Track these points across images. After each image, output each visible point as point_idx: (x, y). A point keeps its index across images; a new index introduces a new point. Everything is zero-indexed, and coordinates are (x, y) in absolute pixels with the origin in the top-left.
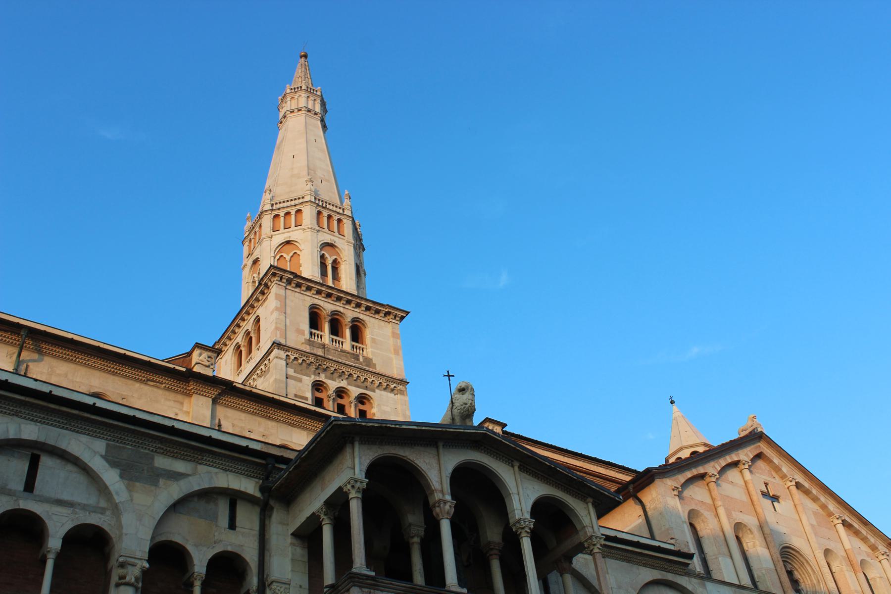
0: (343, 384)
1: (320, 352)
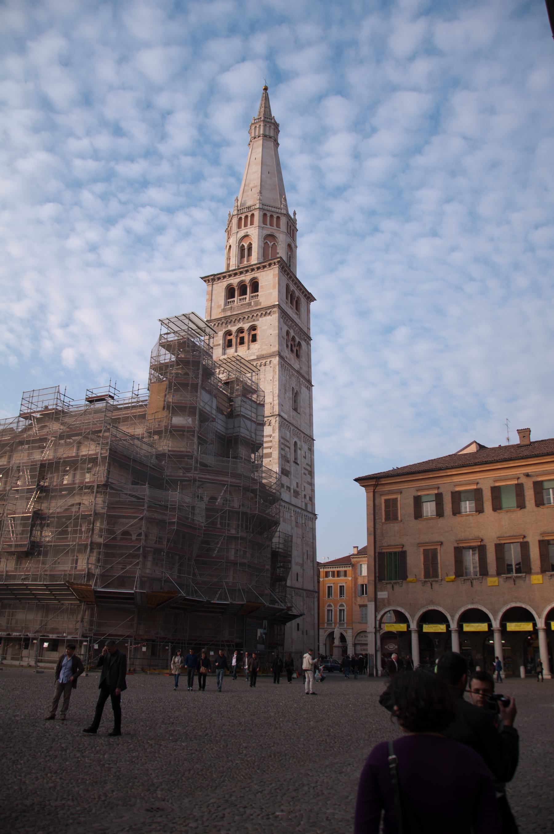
0: (240, 325)
1: (229, 313)
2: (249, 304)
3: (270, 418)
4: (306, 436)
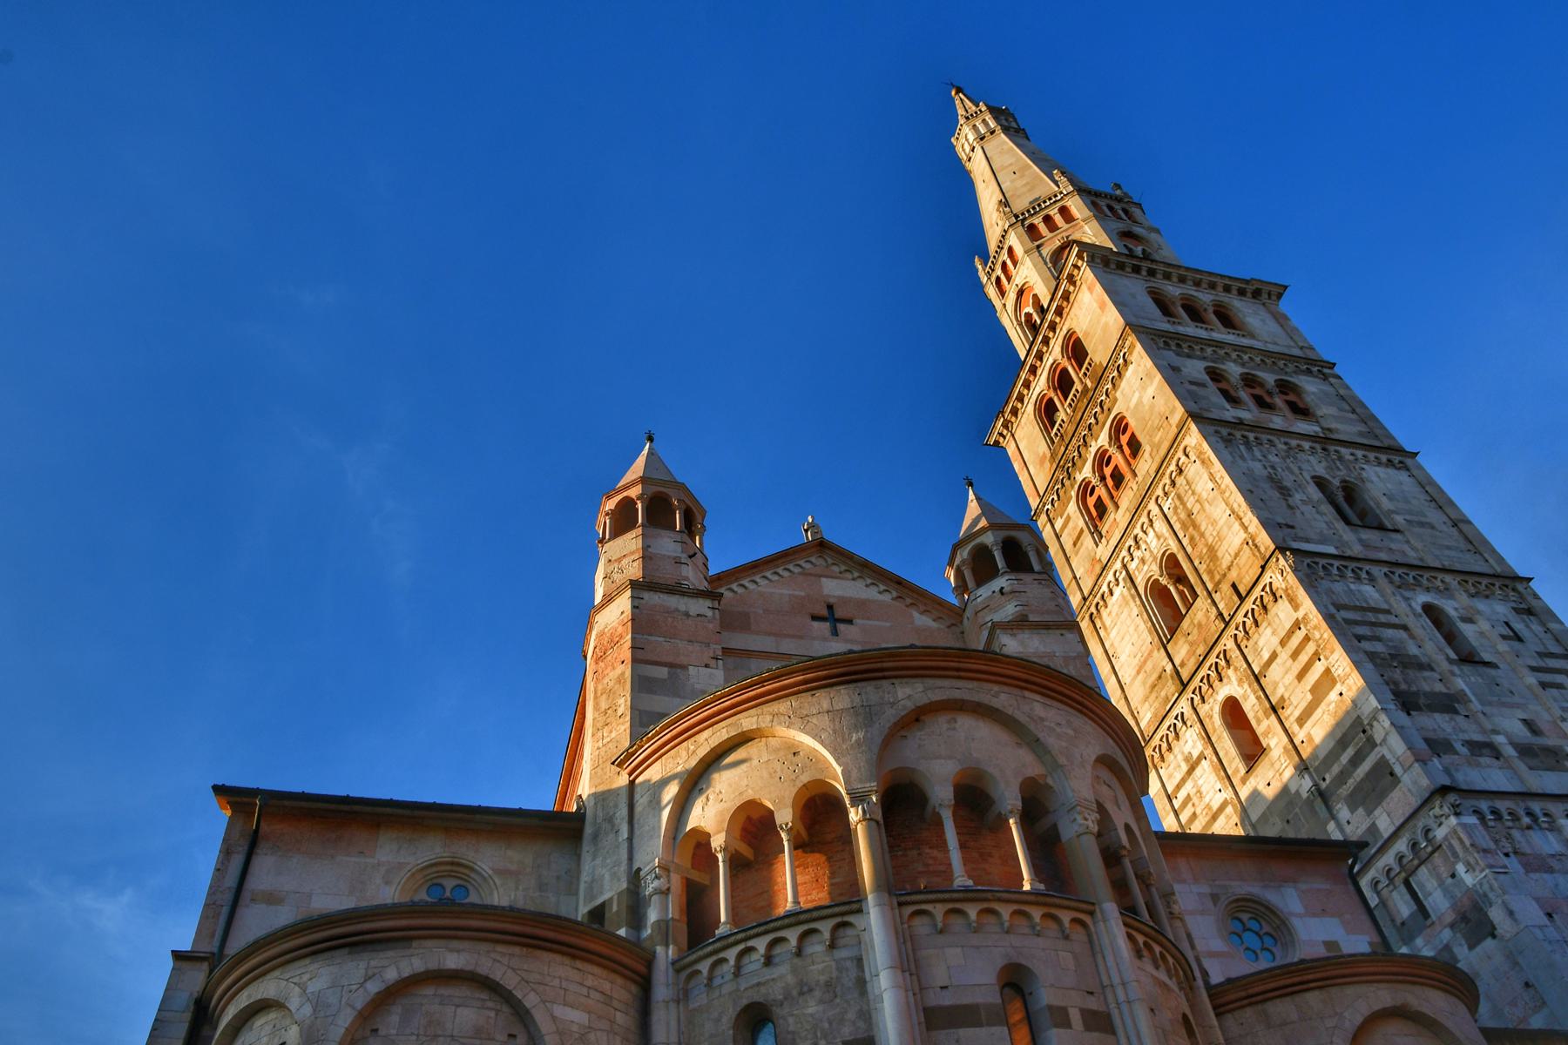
0: (1093, 450)
2: (1086, 389)
3: (1266, 579)
4: (1471, 580)
